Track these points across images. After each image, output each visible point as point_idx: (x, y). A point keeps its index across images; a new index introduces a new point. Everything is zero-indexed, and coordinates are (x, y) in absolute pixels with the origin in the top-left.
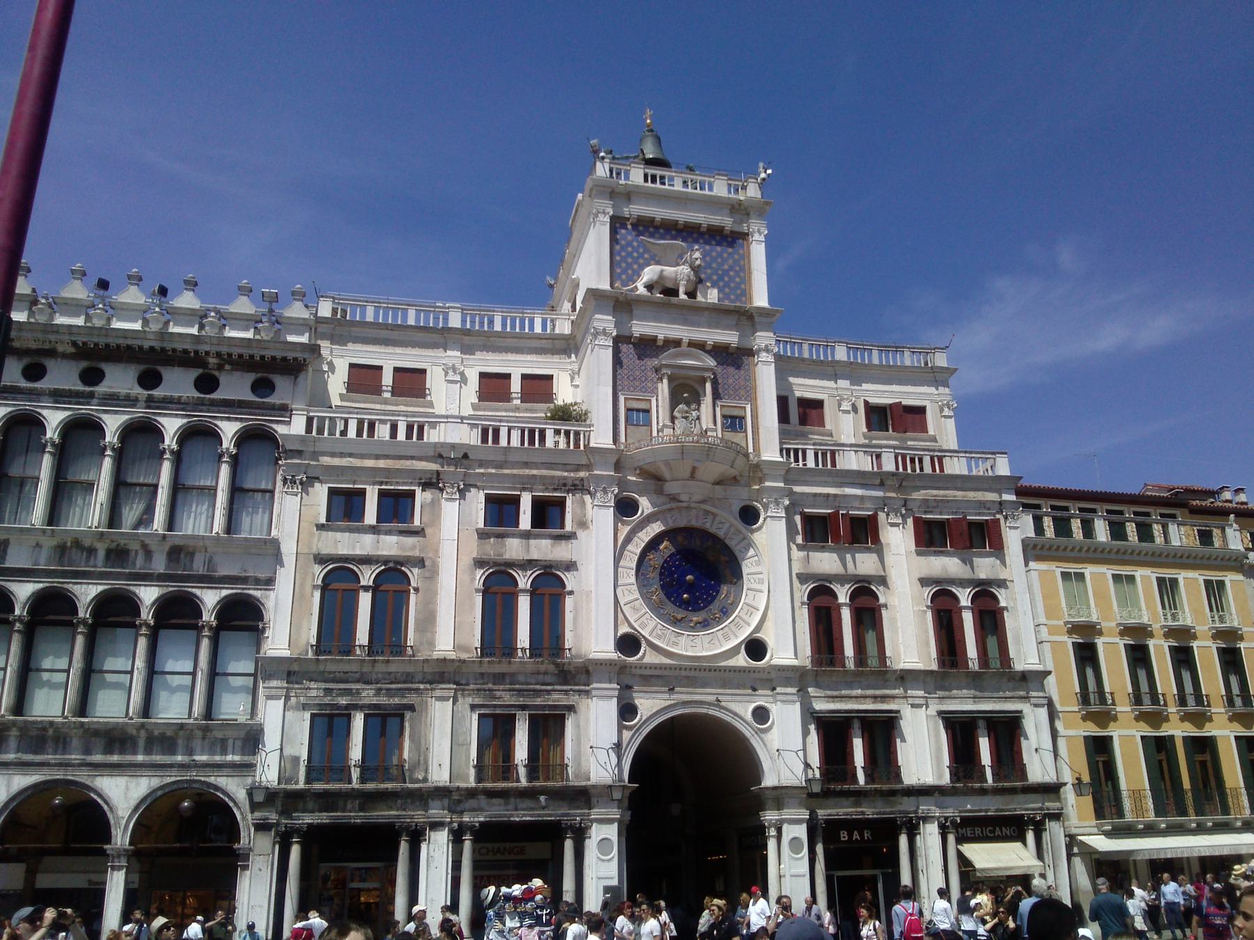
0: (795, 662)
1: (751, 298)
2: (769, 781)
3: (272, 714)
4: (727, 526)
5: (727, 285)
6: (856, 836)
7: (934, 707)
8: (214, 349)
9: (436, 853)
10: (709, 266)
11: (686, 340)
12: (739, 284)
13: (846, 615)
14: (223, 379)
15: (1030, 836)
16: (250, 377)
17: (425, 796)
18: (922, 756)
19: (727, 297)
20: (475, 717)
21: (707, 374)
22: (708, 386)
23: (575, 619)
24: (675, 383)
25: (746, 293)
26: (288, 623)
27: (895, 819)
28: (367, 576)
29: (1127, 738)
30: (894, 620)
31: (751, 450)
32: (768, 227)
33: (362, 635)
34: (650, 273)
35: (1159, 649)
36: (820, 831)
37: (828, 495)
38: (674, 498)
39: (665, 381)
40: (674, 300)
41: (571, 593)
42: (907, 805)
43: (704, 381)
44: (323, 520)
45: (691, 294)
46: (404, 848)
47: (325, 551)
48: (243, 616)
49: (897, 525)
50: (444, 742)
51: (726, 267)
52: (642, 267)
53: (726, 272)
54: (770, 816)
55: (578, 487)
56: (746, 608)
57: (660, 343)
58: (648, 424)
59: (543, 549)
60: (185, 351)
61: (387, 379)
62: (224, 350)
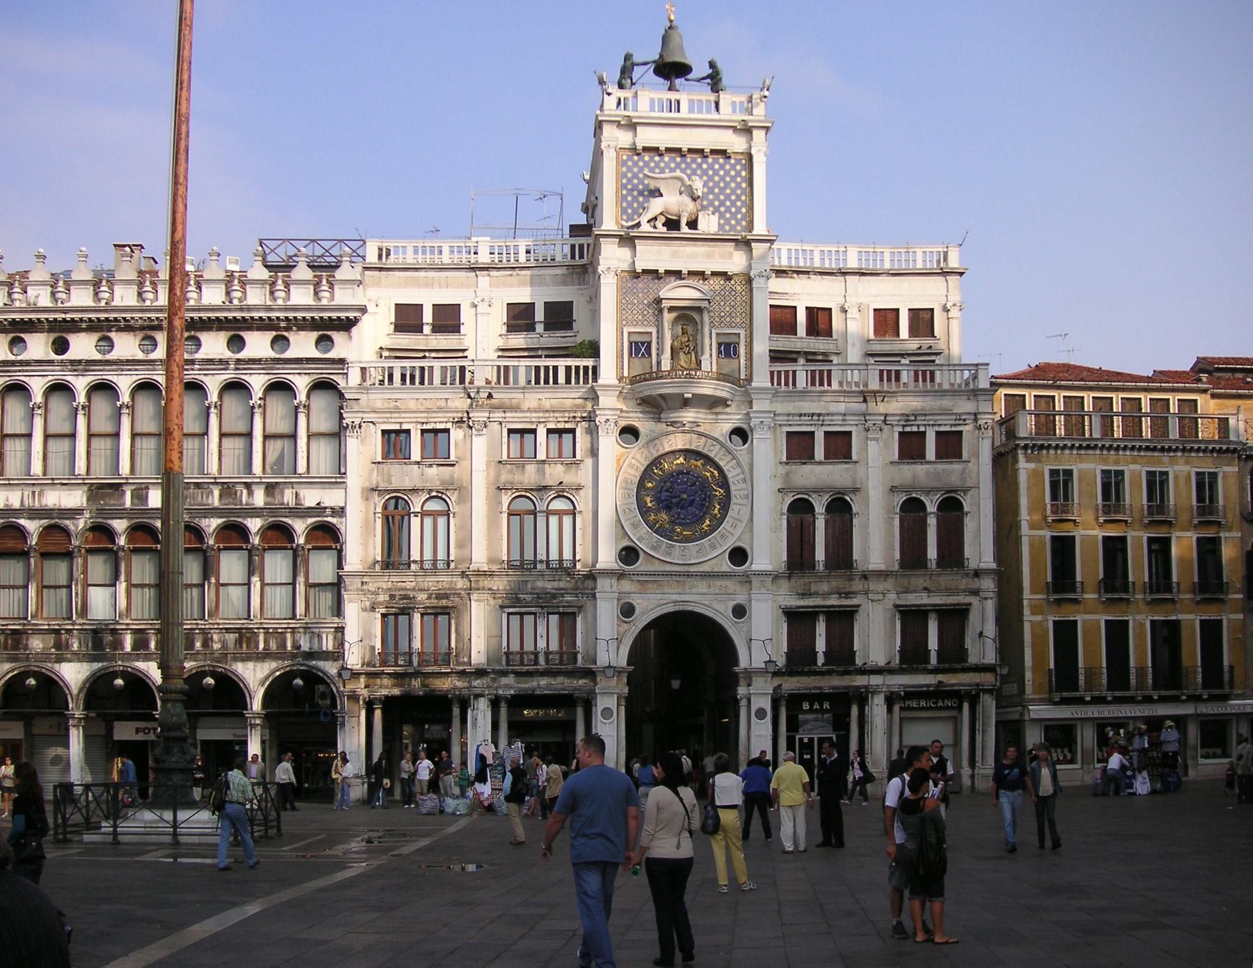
0: (770, 568)
2: (743, 662)
5: (728, 210)
6: (816, 706)
8: (282, 315)
10: (711, 191)
13: (820, 524)
14: (292, 336)
15: (966, 706)
16: (314, 335)
18: (876, 638)
19: (728, 222)
20: (505, 616)
21: (705, 304)
23: (584, 535)
24: (674, 315)
27: (846, 694)
30: (866, 526)
31: (743, 377)
32: (768, 146)
36: (784, 703)
37: (813, 415)
40: (675, 234)
42: (860, 681)
44: (379, 459)
46: (456, 711)
47: (382, 486)
49: (876, 439)
51: (728, 191)
54: (742, 691)
60: (261, 318)
62: (291, 315)
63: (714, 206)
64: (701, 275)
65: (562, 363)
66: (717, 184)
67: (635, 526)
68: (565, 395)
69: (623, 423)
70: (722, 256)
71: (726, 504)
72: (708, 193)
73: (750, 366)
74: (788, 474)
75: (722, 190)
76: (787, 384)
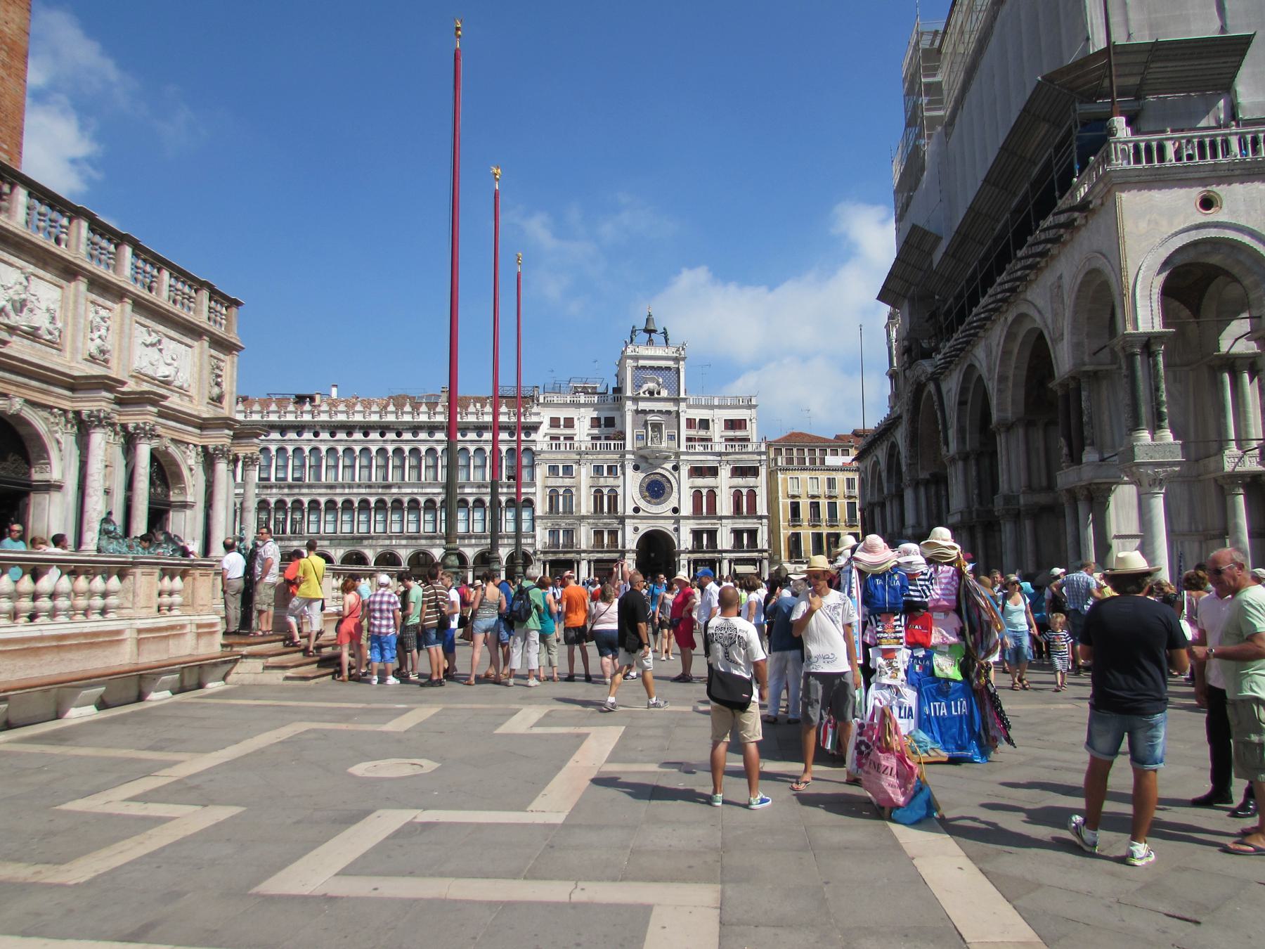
3: (538, 529)
7: (729, 527)
9: (584, 566)
13: (704, 499)
17: (579, 552)
26: (541, 507)
28: (561, 491)
29: (806, 533)
33: (561, 509)
34: (645, 387)
35: (823, 503)
45: (659, 393)
48: (530, 503)
50: (584, 537)
59: (611, 481)
61: (562, 422)
65: (612, 443)
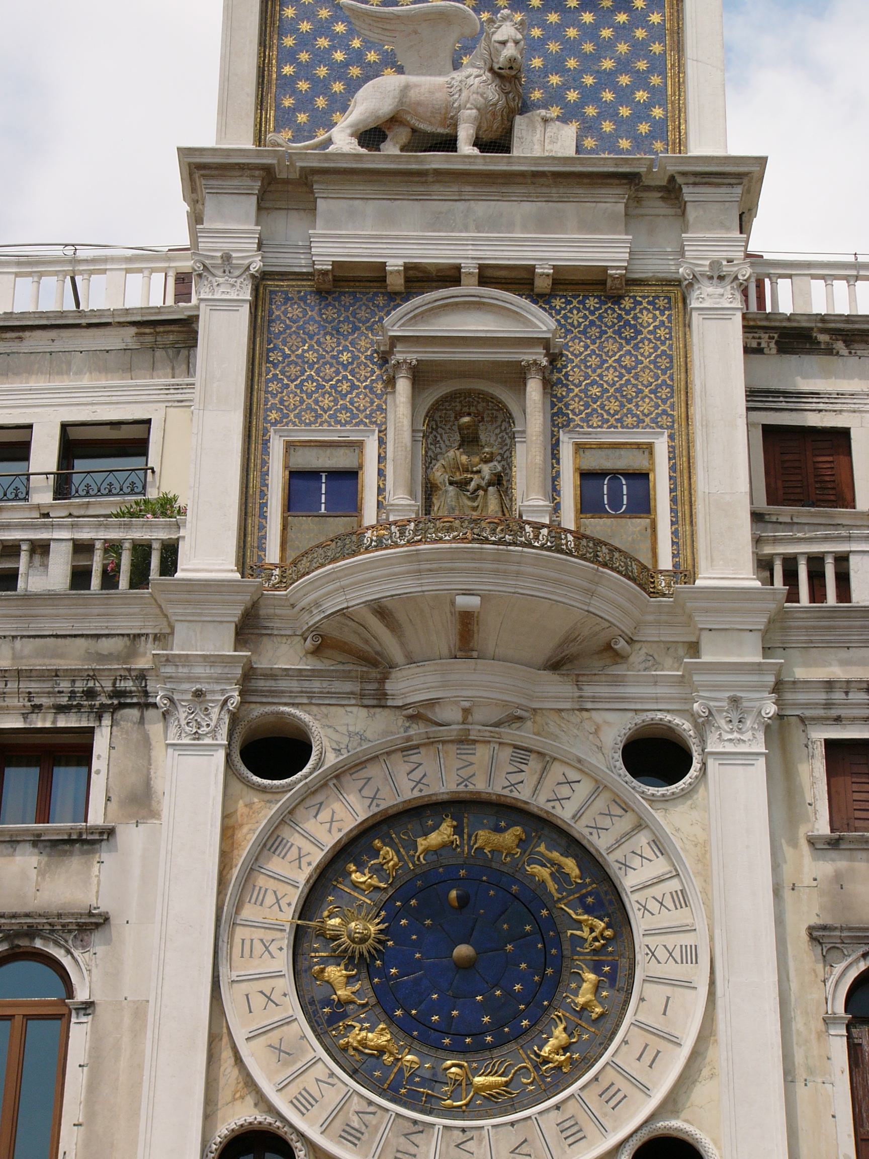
1: (681, 143)
4: (584, 789)
11: (469, 267)
12: (648, 105)
22: (534, 388)
23: (92, 1088)
25: (671, 129)
31: (666, 562)
38: (417, 714)
39: (403, 386)
41: (88, 1007)
43: (517, 376)
51: (608, 64)
52: (353, 86)
53: (607, 80)
55: (128, 699)
56: (638, 1039)
57: (396, 282)
58: (354, 506)
63: (565, 105)
64: (518, 280)
66: (571, 48)
67: (283, 1053)
68: (63, 627)
69: (257, 711)
70: (585, 226)
71: (618, 974)
72: (545, 72)
73: (684, 541)
74: (839, 880)
75: (596, 58)
76: (817, 593)
